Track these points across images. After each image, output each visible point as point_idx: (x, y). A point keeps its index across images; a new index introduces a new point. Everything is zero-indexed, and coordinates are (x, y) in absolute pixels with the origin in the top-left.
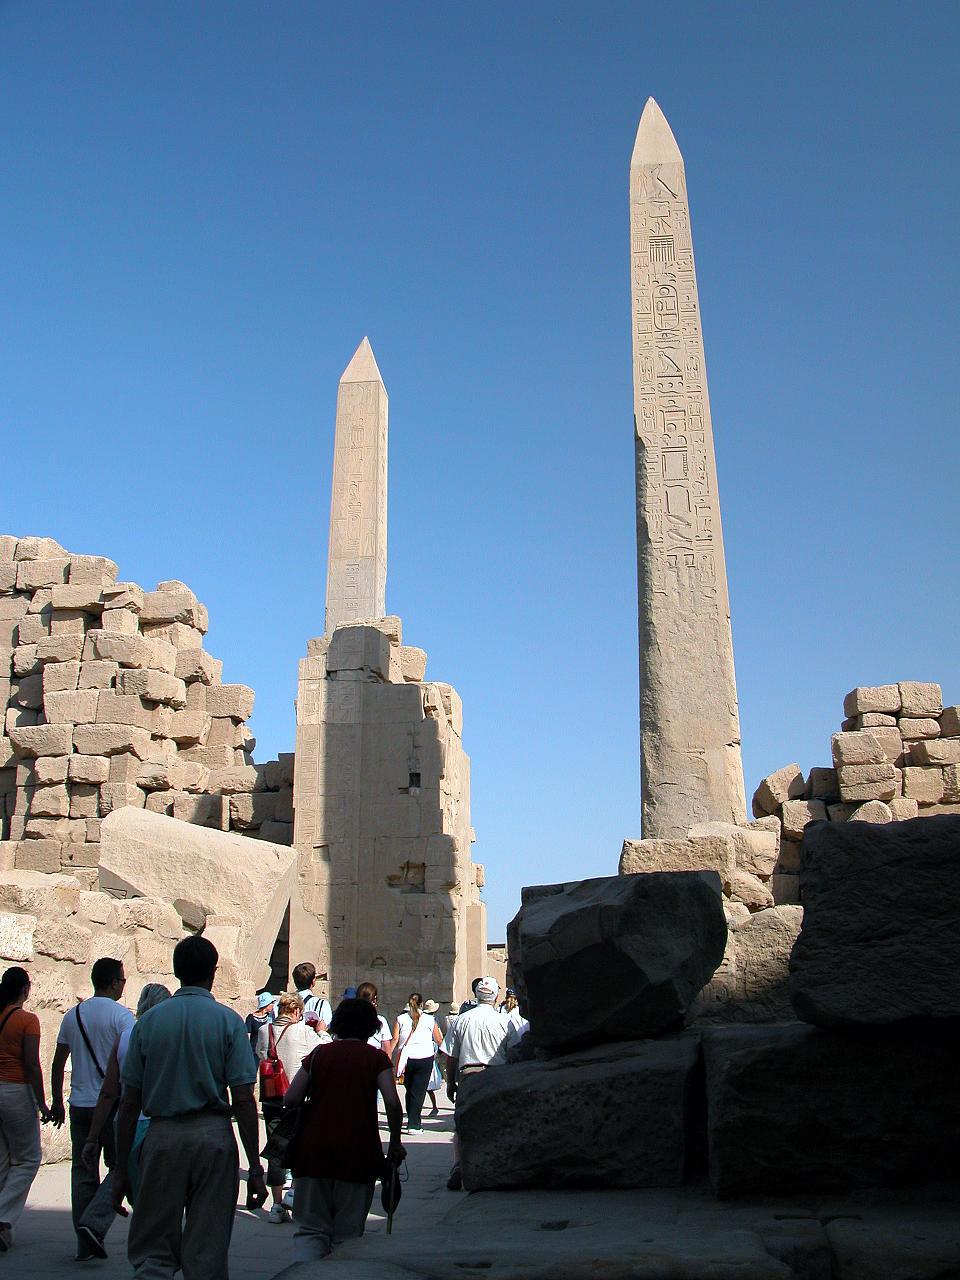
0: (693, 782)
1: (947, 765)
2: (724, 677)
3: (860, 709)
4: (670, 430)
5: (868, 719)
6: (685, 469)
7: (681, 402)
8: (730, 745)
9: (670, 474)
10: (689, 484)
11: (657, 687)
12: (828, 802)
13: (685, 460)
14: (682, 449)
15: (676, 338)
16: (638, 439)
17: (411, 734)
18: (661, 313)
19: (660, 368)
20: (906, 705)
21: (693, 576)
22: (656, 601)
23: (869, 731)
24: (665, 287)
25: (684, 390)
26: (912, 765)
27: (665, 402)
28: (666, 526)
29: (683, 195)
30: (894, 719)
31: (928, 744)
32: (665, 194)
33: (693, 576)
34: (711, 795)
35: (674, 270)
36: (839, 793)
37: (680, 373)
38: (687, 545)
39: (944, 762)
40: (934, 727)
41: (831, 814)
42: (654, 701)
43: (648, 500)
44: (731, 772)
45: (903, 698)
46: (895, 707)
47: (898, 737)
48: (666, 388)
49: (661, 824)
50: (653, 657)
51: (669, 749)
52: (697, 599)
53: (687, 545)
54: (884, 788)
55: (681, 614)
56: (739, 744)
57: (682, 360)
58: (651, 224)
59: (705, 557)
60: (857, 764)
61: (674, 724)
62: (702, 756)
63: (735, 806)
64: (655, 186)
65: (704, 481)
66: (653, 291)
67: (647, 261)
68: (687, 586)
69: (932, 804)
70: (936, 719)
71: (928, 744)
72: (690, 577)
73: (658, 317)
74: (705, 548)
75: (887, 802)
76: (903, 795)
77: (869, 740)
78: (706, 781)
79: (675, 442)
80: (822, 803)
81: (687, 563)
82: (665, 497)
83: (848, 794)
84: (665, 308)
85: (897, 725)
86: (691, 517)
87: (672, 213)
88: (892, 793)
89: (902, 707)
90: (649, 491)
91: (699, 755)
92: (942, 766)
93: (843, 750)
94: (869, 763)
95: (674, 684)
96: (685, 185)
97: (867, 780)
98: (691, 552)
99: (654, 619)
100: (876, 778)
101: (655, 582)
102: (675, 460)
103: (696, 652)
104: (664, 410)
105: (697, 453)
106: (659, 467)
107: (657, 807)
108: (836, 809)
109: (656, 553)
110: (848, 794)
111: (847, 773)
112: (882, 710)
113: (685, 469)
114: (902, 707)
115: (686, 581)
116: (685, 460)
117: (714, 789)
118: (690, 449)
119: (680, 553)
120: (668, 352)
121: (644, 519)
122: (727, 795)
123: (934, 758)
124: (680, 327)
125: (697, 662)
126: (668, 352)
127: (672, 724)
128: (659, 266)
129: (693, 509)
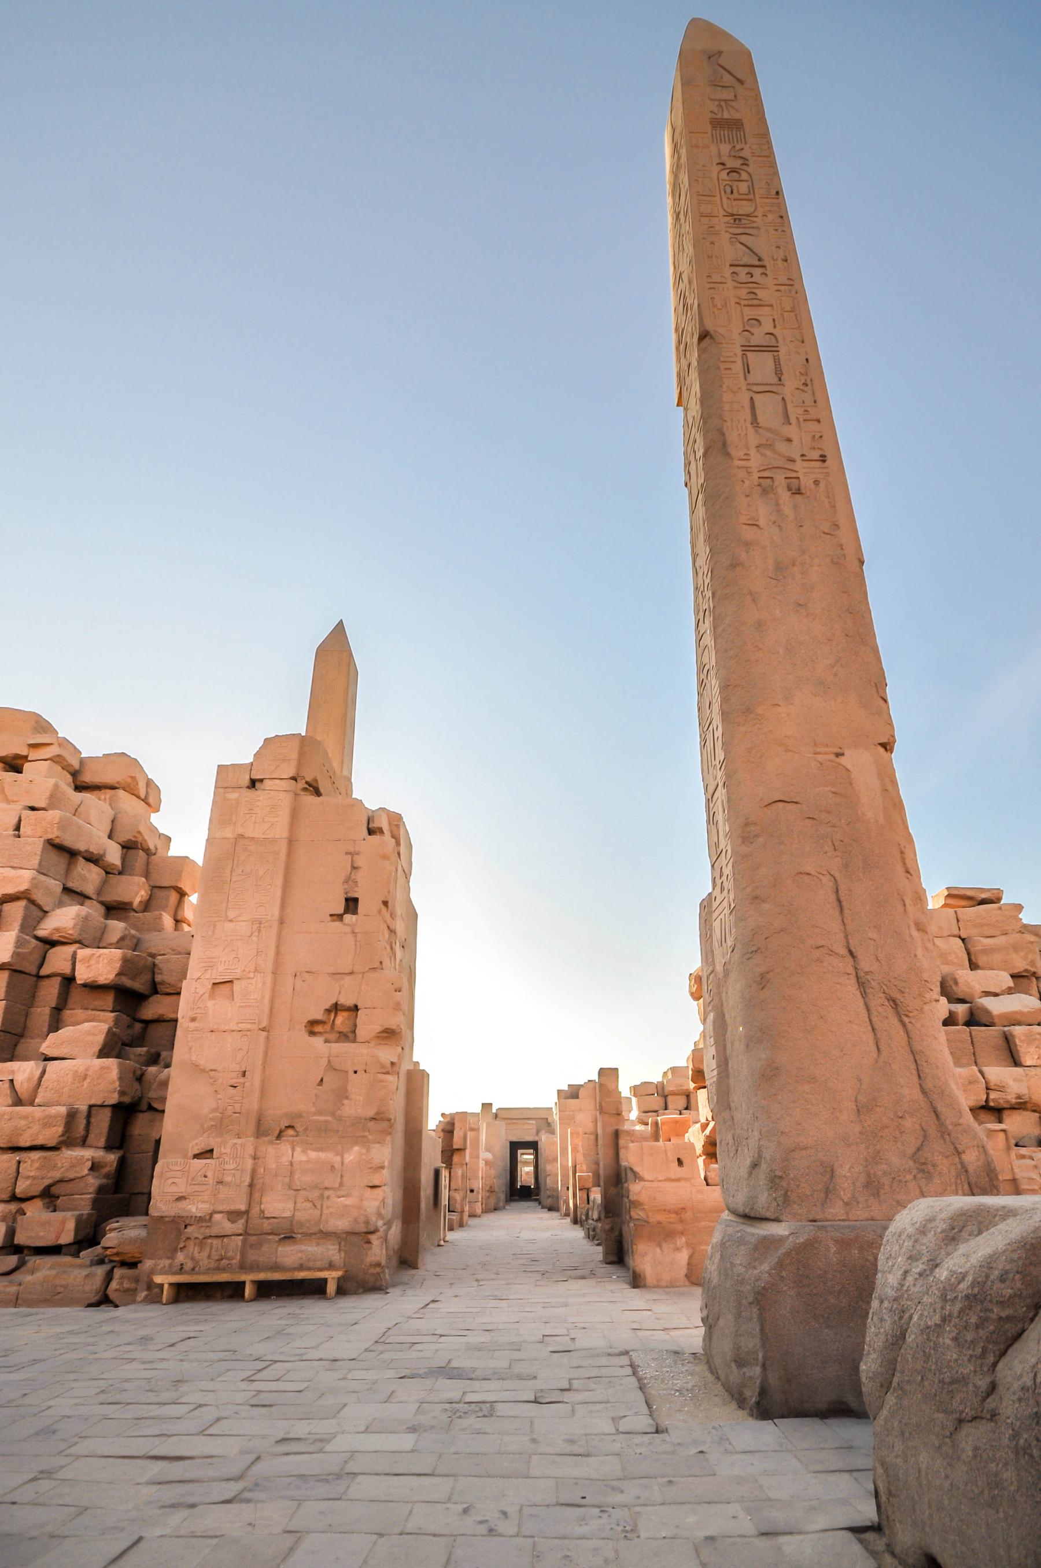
6: (779, 372)
9: (756, 376)
13: (777, 362)
15: (754, 225)
17: (350, 853)
18: (730, 196)
24: (733, 170)
27: (743, 293)
35: (746, 153)
48: (743, 276)
58: (713, 106)
59: (816, 483)
62: (842, 760)
65: (808, 389)
72: (796, 508)
73: (725, 201)
79: (758, 337)
84: (735, 191)
86: (791, 431)
91: (832, 757)
102: (762, 366)
106: (738, 367)
113: (779, 372)
115: (787, 510)
116: (777, 362)
126: (743, 239)
128: (725, 148)
129: (793, 421)
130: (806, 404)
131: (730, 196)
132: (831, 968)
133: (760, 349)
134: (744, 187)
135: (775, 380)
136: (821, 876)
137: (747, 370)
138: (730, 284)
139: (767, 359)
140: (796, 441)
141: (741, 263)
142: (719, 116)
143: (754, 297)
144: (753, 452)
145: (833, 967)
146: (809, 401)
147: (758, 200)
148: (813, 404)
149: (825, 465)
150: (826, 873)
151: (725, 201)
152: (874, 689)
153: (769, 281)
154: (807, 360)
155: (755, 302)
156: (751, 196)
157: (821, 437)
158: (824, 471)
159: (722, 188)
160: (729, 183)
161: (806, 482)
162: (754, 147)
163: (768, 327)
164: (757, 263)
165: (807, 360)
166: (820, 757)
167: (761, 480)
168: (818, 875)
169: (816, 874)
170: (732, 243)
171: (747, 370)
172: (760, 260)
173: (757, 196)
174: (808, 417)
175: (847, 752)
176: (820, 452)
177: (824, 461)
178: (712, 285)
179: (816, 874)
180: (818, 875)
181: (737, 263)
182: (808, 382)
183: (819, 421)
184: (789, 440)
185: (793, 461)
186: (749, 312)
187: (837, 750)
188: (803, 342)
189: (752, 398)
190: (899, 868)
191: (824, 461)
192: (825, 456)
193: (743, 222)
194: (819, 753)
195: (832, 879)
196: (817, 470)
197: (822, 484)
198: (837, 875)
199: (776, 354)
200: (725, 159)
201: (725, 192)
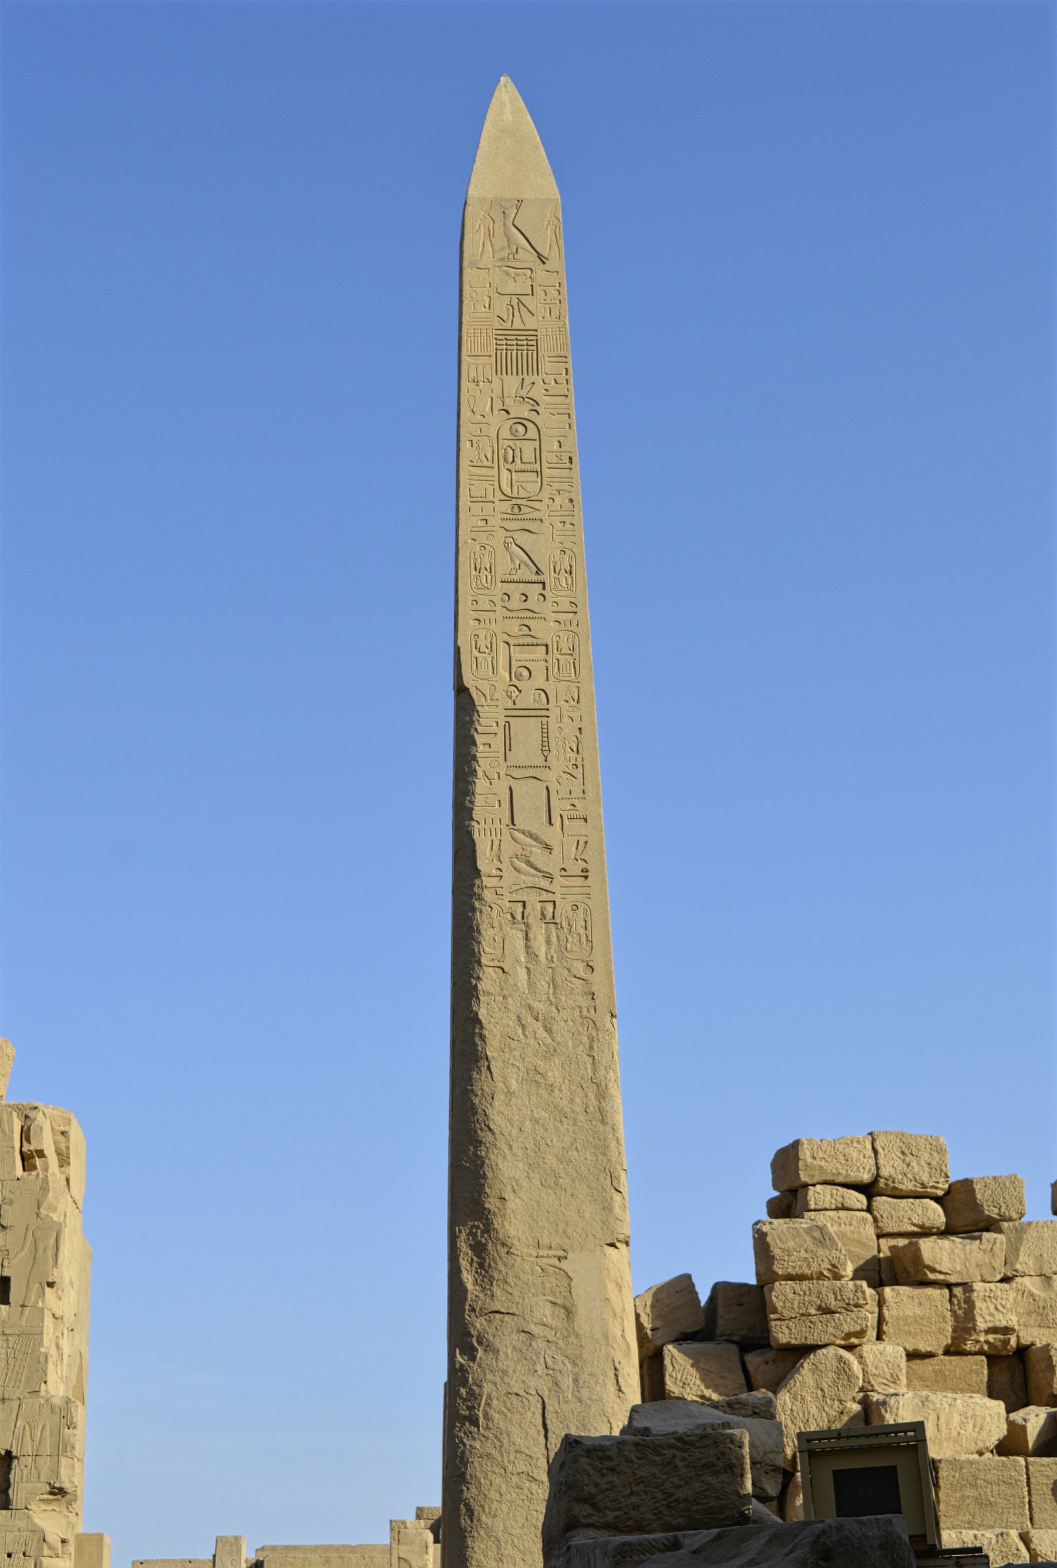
0: (545, 1311)
1: (957, 1285)
2: (603, 1122)
3: (804, 1177)
4: (519, 677)
5: (818, 1195)
6: (545, 747)
7: (545, 630)
8: (612, 1245)
9: (518, 755)
10: (551, 777)
11: (485, 1136)
12: (745, 1347)
13: (545, 731)
14: (540, 713)
15: (536, 515)
16: (461, 691)
19: (504, 566)
20: (885, 1172)
21: (554, 940)
22: (488, 981)
23: (822, 1219)
24: (521, 421)
25: (546, 608)
26: (895, 1282)
27: (514, 627)
28: (509, 849)
29: (556, 260)
30: (863, 1198)
31: (928, 1248)
32: (527, 257)
33: (554, 940)
34: (578, 1336)
35: (538, 393)
36: (767, 1330)
37: (540, 578)
38: (544, 883)
39: (953, 1279)
40: (936, 1215)
41: (751, 1368)
42: (479, 1163)
43: (479, 800)
44: (612, 1292)
45: (881, 1161)
46: (866, 1177)
47: (870, 1231)
48: (516, 602)
49: (487, 1388)
50: (481, 1082)
51: (504, 1250)
52: (559, 981)
53: (544, 883)
54: (848, 1323)
55: (530, 1007)
56: (627, 1244)
57: (545, 551)
58: (501, 306)
60: (800, 1278)
61: (513, 1203)
62: (564, 1265)
63: (618, 1357)
64: (507, 234)
65: (578, 773)
66: (498, 422)
67: (489, 372)
68: (542, 957)
69: (930, 1355)
70: (937, 1199)
71: (928, 1248)
72: (548, 942)
73: (505, 474)
74: (575, 890)
75: (850, 1348)
76: (879, 1338)
77: (822, 1236)
78: (569, 1312)
79: (528, 699)
80: (734, 1348)
81: (542, 914)
82: (508, 796)
83: (783, 1334)
84: (518, 460)
85: (869, 1209)
86: (552, 835)
87: (539, 291)
88: (861, 1334)
89: (878, 1176)
90: (481, 785)
91: (555, 1262)
92: (949, 1286)
93: (776, 1252)
94: (821, 1276)
95: (515, 1132)
96: (562, 241)
97: (819, 1308)
98: (550, 897)
99: (483, 1013)
100: (833, 1304)
101: (488, 949)
103: (554, 1074)
104: (512, 641)
105: (566, 720)
106: (498, 743)
107: (480, 1353)
108: (759, 1359)
109: (488, 895)
110: (783, 1334)
111: (782, 1294)
112: (841, 1179)
113: (545, 747)
114: (878, 1176)
116: (545, 731)
117: (582, 1323)
118: (554, 713)
119: (533, 899)
120: (522, 538)
121: (470, 834)
122: (606, 1337)
123: (933, 1270)
124: (545, 495)
125: (557, 1092)
126: (522, 538)
127: (510, 1205)
128: (512, 382)
129: (556, 820)
130: (573, 795)
131: (511, 467)
132: (530, 1495)
133: (527, 712)
134: (528, 450)
135: (540, 761)
136: (530, 1398)
137: (508, 746)
138: (500, 612)
139: (534, 724)
140: (557, 850)
141: (515, 578)
142: (508, 325)
143: (528, 632)
144: (505, 866)
145: (532, 1494)
146: (577, 792)
147: (546, 471)
148: (581, 795)
149: (588, 882)
150: (535, 1393)
151: (505, 474)
152: (609, 1178)
153: (546, 608)
154: (580, 729)
155: (529, 640)
156: (537, 467)
157: (586, 842)
158: (585, 890)
159: (502, 452)
160: (511, 443)
161: (564, 907)
162: (550, 379)
163: (539, 681)
164: (535, 578)
165: (580, 729)
166: (542, 1262)
167: (511, 904)
168: (526, 1396)
169: (524, 1394)
170: (506, 546)
171: (508, 746)
172: (538, 572)
173: (545, 464)
174: (574, 814)
175: (570, 1255)
176: (584, 865)
177: (586, 877)
178: (475, 615)
179: (524, 1394)
180: (526, 1396)
181: (511, 578)
182: (579, 764)
183: (586, 820)
184: (548, 848)
185: (550, 877)
186: (517, 654)
187: (561, 1253)
188: (578, 702)
189: (511, 789)
190: (612, 1387)
191: (586, 877)
192: (587, 871)
193: (524, 509)
194: (542, 1257)
195: (540, 1400)
196: (575, 890)
197: (580, 911)
198: (545, 1394)
199: (544, 720)
200: (509, 403)
201: (505, 460)
